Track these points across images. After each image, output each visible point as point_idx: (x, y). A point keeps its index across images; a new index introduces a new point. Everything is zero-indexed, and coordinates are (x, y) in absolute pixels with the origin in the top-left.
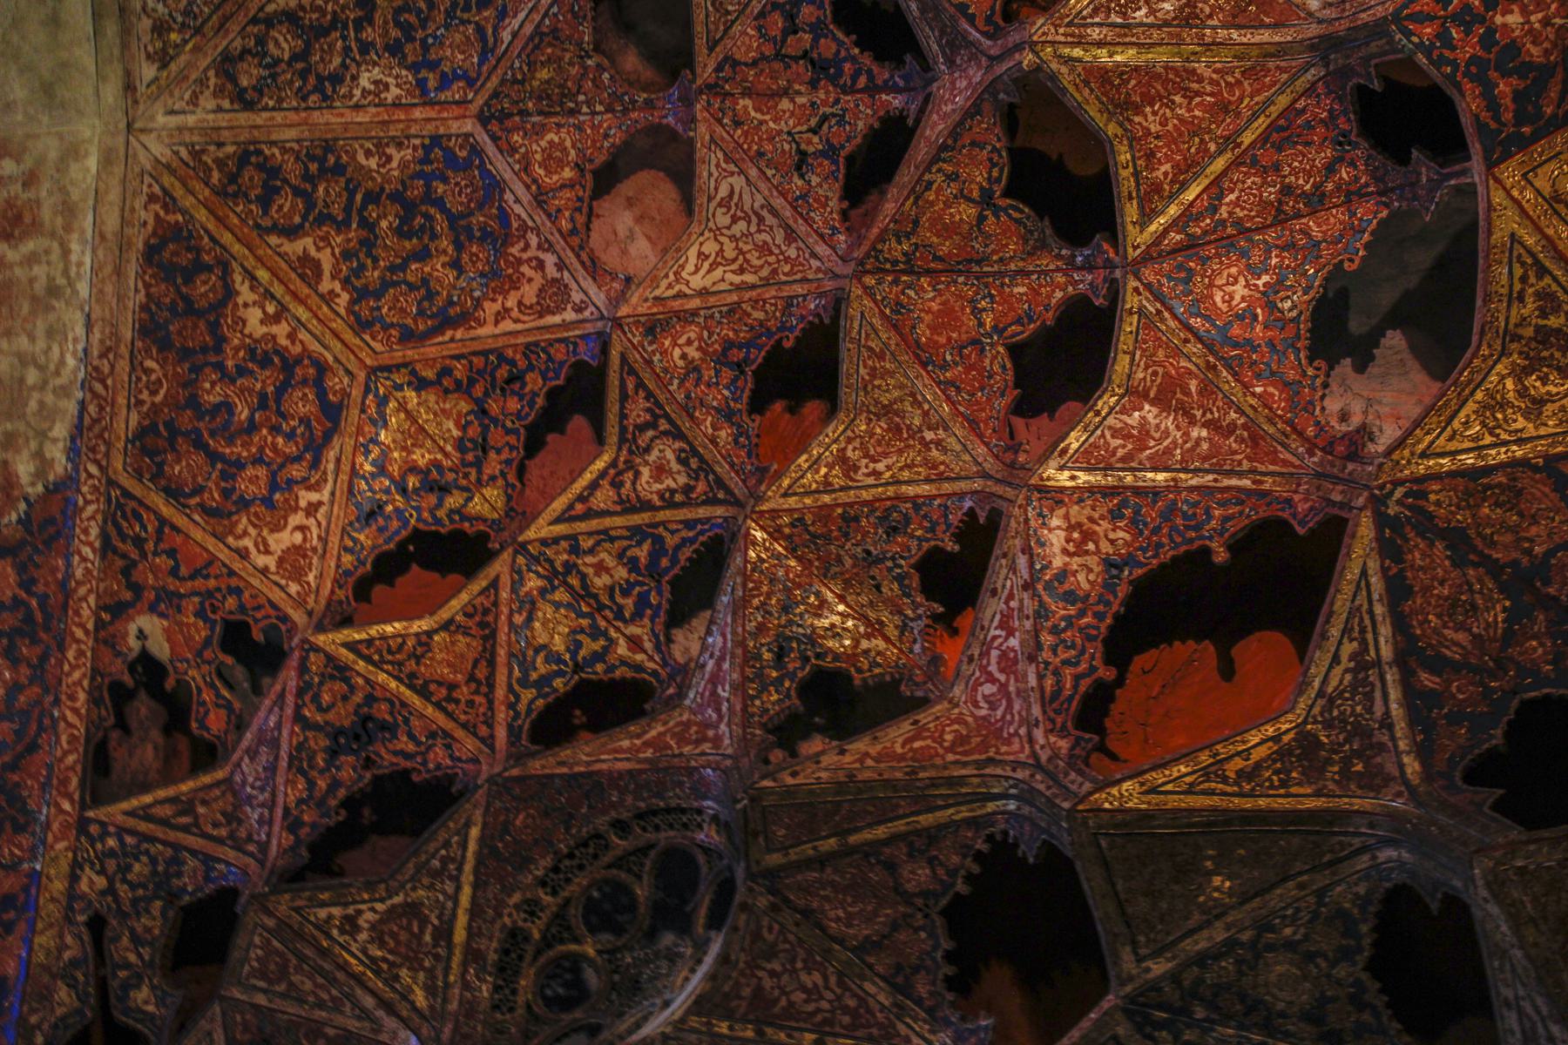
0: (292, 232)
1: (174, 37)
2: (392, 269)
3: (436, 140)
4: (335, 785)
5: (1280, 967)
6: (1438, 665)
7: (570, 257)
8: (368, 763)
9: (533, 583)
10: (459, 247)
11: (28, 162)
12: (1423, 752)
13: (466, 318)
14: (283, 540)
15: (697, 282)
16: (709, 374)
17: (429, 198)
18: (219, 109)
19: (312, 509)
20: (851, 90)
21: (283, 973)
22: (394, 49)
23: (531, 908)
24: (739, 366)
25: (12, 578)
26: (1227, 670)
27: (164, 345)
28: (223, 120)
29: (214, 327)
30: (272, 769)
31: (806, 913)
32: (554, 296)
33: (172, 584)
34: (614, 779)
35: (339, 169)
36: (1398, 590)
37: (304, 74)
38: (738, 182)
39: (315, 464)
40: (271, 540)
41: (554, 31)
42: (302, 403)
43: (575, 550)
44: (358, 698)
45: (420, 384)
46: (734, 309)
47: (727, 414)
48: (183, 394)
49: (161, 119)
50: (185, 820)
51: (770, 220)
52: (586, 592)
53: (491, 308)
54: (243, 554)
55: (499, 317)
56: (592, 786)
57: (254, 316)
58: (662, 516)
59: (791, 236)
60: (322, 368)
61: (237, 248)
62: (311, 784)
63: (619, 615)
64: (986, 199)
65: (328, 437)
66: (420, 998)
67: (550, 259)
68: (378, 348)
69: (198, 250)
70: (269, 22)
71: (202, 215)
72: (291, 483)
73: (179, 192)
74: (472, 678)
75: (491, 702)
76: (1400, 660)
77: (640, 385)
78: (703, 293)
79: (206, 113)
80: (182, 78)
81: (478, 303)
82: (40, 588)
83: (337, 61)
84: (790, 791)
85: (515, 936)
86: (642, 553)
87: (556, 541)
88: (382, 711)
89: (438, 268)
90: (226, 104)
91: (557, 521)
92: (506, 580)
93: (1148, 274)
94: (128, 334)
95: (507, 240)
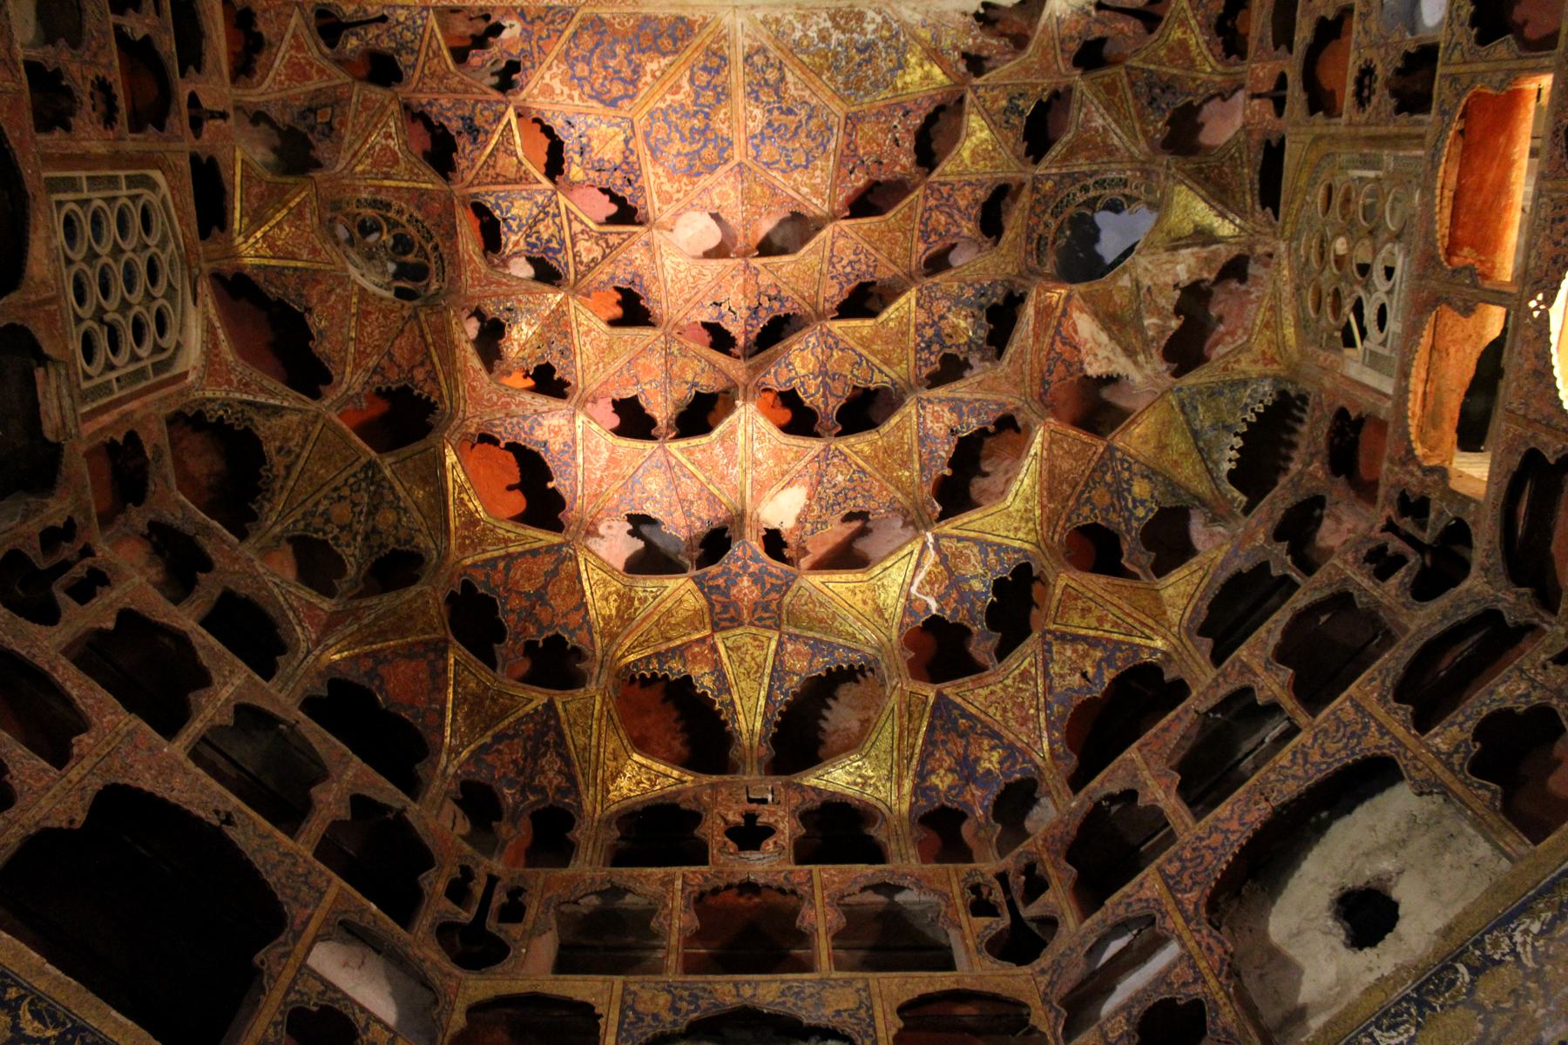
0: (692, 80)
2: (676, 126)
3: (731, 144)
4: (449, 119)
5: (391, 517)
6: (508, 568)
7: (681, 204)
8: (459, 133)
9: (540, 199)
12: (474, 565)
13: (655, 159)
14: (557, 85)
15: (668, 263)
16: (630, 269)
17: (707, 141)
19: (571, 97)
20: (746, 324)
21: (366, 109)
22: (770, 124)
23: (400, 212)
26: (510, 488)
27: (640, 27)
29: (650, 49)
30: (455, 91)
31: (402, 331)
32: (667, 199)
33: (535, 37)
34: (455, 245)
35: (719, 101)
36: (534, 553)
37: (759, 84)
39: (590, 97)
42: (617, 89)
43: (554, 216)
45: (626, 141)
46: (656, 278)
47: (612, 278)
49: (739, 21)
52: (536, 222)
53: (660, 170)
54: (549, 68)
55: (657, 175)
56: (451, 233)
59: (687, 301)
60: (632, 98)
63: (528, 236)
64: (695, 385)
65: (602, 102)
66: (359, 168)
68: (641, 121)
70: (780, 69)
73: (708, 30)
76: (509, 555)
78: (663, 265)
79: (742, 44)
80: (757, 30)
84: (449, 323)
85: (388, 206)
86: (554, 245)
88: (481, 138)
89: (677, 146)
93: (660, 452)
94: (645, 11)
95: (690, 175)
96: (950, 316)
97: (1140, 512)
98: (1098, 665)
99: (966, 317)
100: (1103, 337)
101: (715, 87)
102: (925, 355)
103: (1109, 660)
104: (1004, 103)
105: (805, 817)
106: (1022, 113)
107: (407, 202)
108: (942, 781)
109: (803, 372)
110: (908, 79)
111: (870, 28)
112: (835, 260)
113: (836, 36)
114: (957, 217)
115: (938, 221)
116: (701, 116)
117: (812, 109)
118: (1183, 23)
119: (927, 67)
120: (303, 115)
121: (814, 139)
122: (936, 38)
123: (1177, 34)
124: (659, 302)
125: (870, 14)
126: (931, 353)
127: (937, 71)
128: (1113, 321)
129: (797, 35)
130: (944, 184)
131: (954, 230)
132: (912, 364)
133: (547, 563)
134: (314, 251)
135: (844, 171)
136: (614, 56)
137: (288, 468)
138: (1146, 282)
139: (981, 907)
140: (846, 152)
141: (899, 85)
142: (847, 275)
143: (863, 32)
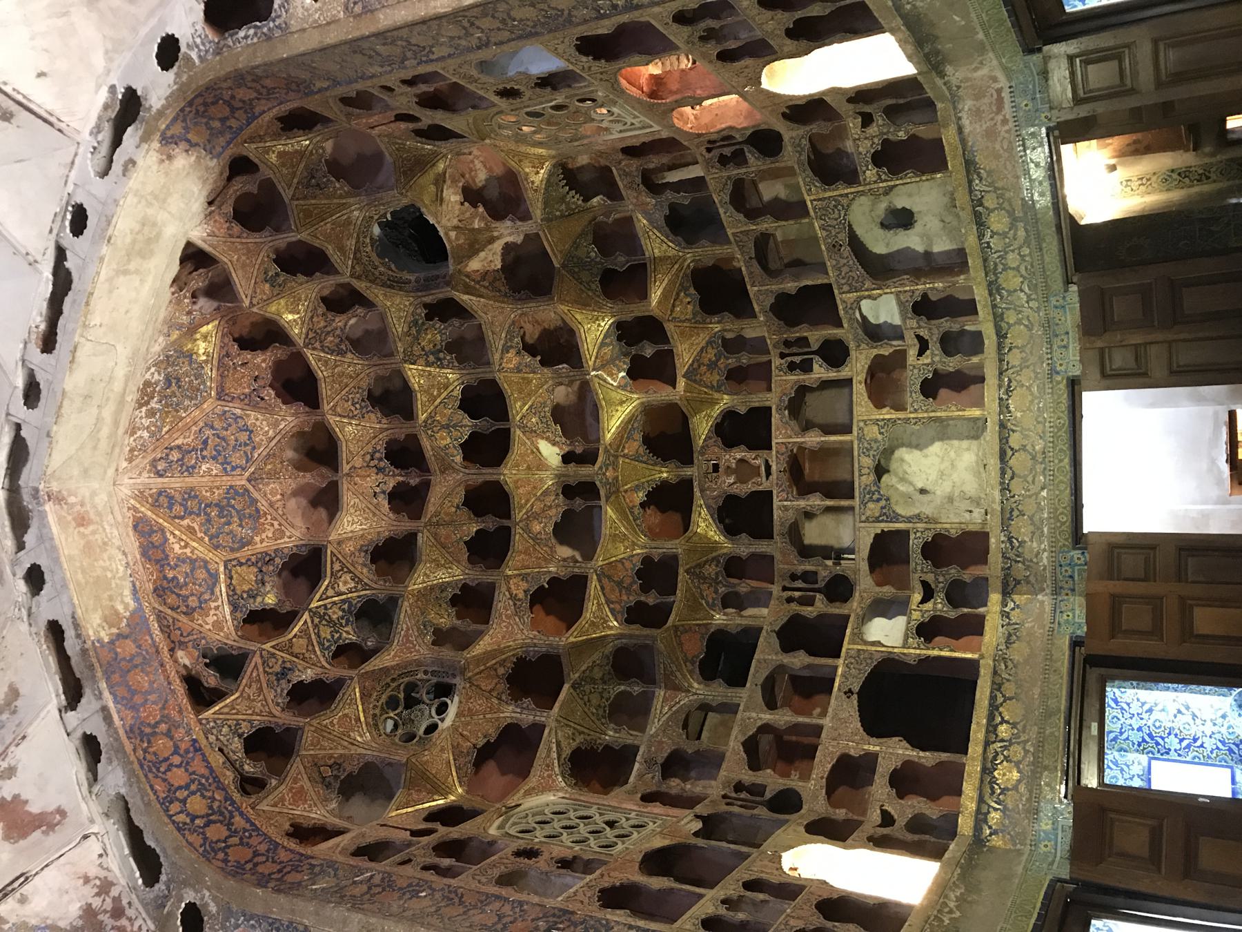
0: (182, 518)
1: (136, 453)
2: (219, 528)
3: (231, 487)
4: (282, 691)
6: (612, 603)
7: (283, 522)
8: (289, 681)
9: (316, 620)
10: (240, 520)
11: (80, 498)
14: (211, 619)
15: (349, 529)
16: (357, 554)
17: (229, 505)
18: (149, 477)
19: (217, 608)
21: (319, 742)
22: (214, 458)
24: (366, 552)
25: (133, 646)
28: (151, 481)
29: (163, 551)
30: (260, 689)
31: (477, 686)
33: (182, 639)
34: (392, 667)
35: (196, 496)
36: (603, 588)
37: (182, 466)
38: (357, 500)
39: (212, 593)
40: (207, 619)
41: (274, 454)
43: (326, 608)
44: (280, 662)
45: (241, 564)
47: (364, 565)
48: (161, 575)
49: (126, 481)
50: (234, 711)
51: (367, 510)
52: (330, 621)
53: (257, 539)
55: (262, 541)
56: (386, 671)
57: (176, 547)
58: (349, 595)
59: (374, 514)
60: (206, 562)
61: (165, 524)
62: (276, 691)
63: (341, 625)
64: (458, 507)
65: (214, 585)
66: (359, 738)
67: (276, 523)
69: (151, 526)
70: (171, 449)
71: (149, 513)
72: (206, 601)
74: (308, 650)
75: (317, 656)
76: (606, 603)
77: (338, 559)
78: (352, 532)
80: (137, 466)
81: (252, 538)
82: (144, 647)
83: (193, 461)
84: (474, 656)
85: (375, 715)
86: (346, 606)
87: (320, 606)
88: (288, 665)
89: (234, 526)
90: (152, 475)
91: (318, 601)
92: (309, 621)
93: (521, 524)
94: (138, 557)
95: (259, 517)
96: (423, 344)
97: (593, 254)
98: (687, 295)
99: (426, 334)
100: (482, 254)
101: (184, 499)
102: (445, 362)
103: (686, 289)
104: (267, 286)
105: (729, 444)
106: (277, 274)
107: (369, 704)
108: (715, 378)
109: (449, 439)
110: (201, 351)
111: (156, 376)
112: (351, 415)
113: (154, 404)
114: (329, 329)
115: (331, 342)
116: (208, 510)
117: (206, 425)
118: (267, 151)
119: (198, 336)
120: (328, 786)
121: (230, 425)
122: (180, 327)
123: (273, 158)
124: (379, 533)
125: (148, 376)
126: (445, 358)
127: (204, 329)
128: (473, 248)
129: (146, 434)
130: (307, 334)
131: (338, 332)
132: (449, 371)
133: (605, 581)
134: (442, 750)
135: (262, 404)
136: (175, 578)
137: (581, 733)
138: (455, 222)
139: (806, 367)
140: (246, 401)
141: (204, 358)
142: (362, 408)
143: (157, 383)
